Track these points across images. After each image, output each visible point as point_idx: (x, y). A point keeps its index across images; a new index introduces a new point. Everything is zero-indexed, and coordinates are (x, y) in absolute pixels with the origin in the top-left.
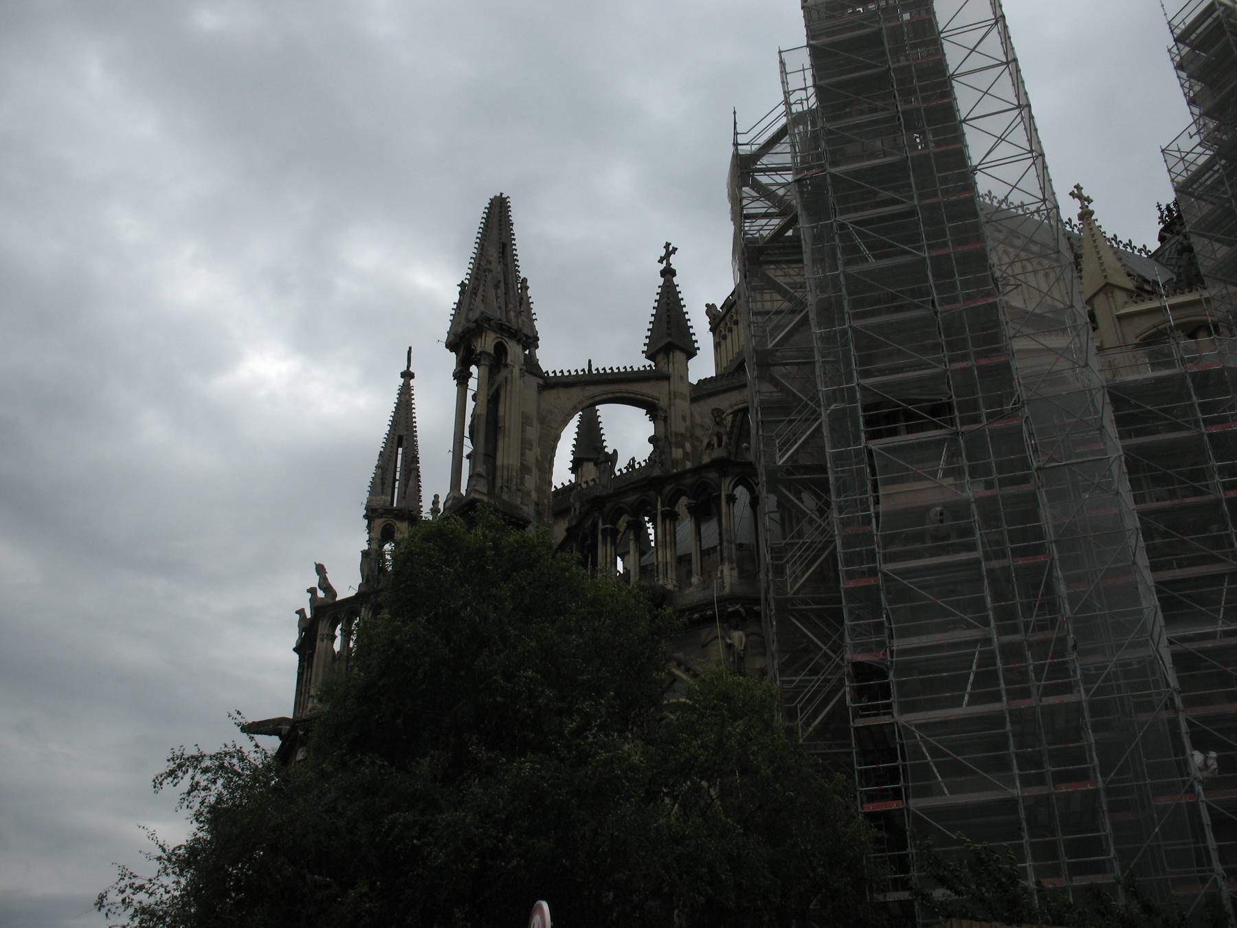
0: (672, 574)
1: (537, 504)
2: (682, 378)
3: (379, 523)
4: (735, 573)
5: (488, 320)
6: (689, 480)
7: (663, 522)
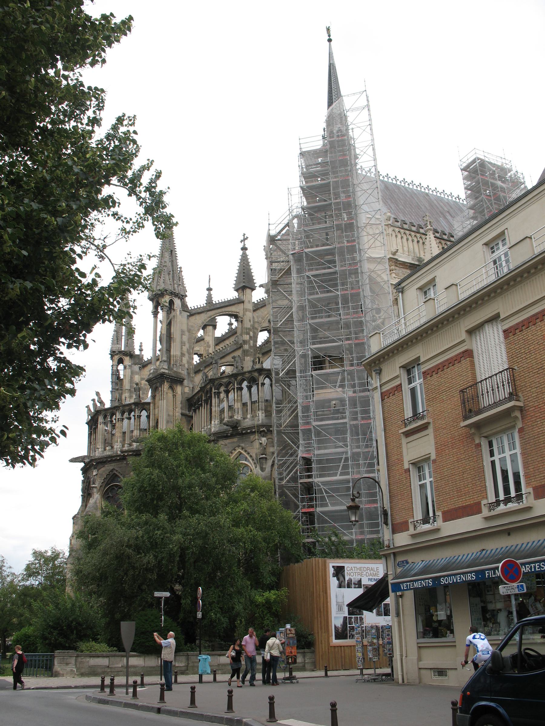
0: (240, 412)
1: (188, 369)
2: (249, 301)
3: (116, 358)
4: (264, 415)
5: (166, 290)
6: (247, 375)
7: (237, 391)
